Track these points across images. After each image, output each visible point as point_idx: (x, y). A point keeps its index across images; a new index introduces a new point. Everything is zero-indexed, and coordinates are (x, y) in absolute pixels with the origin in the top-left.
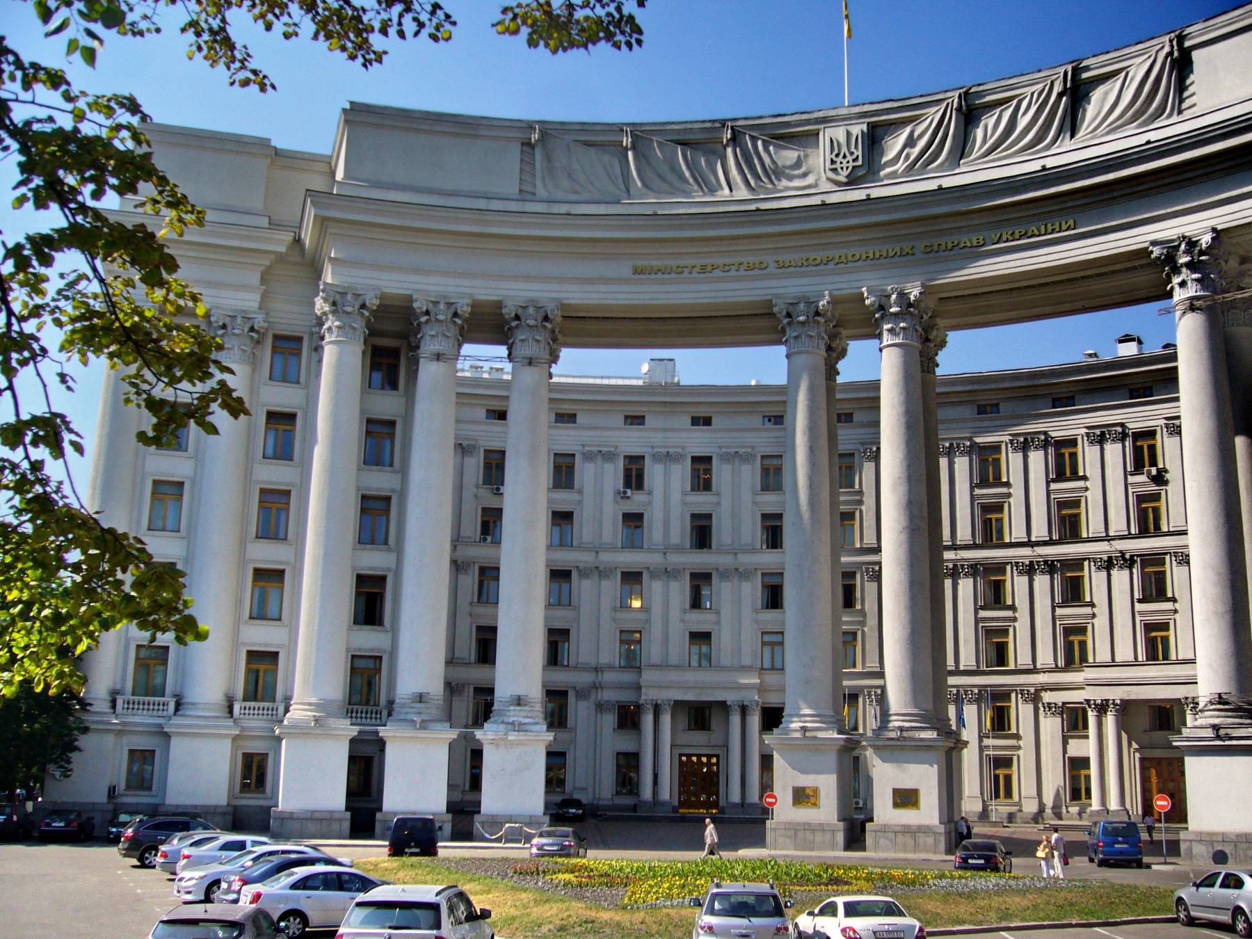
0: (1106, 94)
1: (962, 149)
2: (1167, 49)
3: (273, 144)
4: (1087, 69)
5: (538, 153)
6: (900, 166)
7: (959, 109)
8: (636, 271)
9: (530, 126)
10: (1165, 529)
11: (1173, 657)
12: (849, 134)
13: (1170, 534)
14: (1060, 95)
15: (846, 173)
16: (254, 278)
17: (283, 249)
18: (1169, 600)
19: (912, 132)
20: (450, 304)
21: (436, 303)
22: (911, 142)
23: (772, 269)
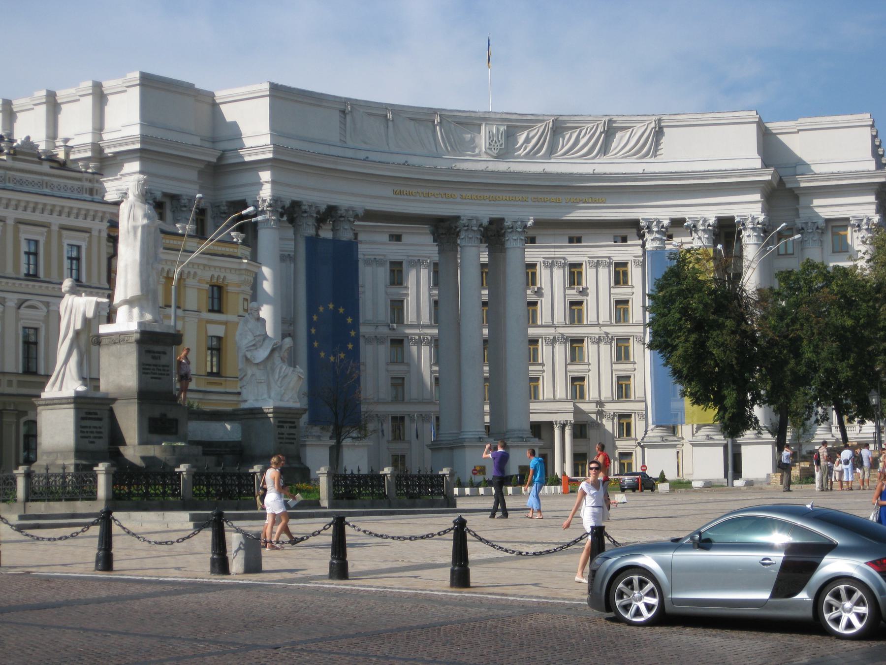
0: (622, 137)
1: (552, 150)
2: (653, 125)
3: (197, 86)
4: (615, 122)
5: (348, 118)
6: (522, 152)
7: (552, 128)
8: (395, 193)
9: (346, 101)
10: (539, 323)
11: (541, 398)
12: (498, 130)
13: (542, 326)
14: (601, 133)
15: (496, 152)
16: (193, 175)
17: (214, 160)
18: (540, 364)
19: (528, 134)
20: (316, 207)
21: (310, 206)
22: (527, 140)
23: (459, 200)
